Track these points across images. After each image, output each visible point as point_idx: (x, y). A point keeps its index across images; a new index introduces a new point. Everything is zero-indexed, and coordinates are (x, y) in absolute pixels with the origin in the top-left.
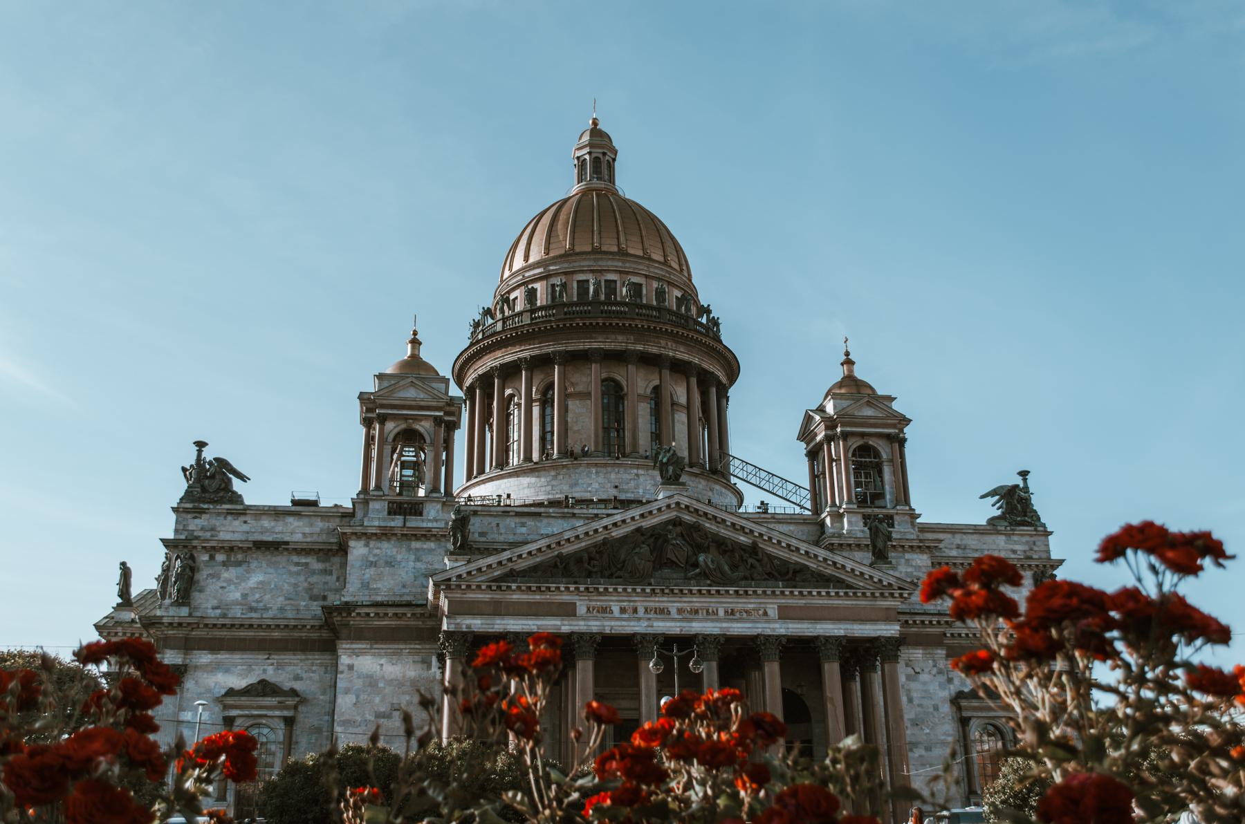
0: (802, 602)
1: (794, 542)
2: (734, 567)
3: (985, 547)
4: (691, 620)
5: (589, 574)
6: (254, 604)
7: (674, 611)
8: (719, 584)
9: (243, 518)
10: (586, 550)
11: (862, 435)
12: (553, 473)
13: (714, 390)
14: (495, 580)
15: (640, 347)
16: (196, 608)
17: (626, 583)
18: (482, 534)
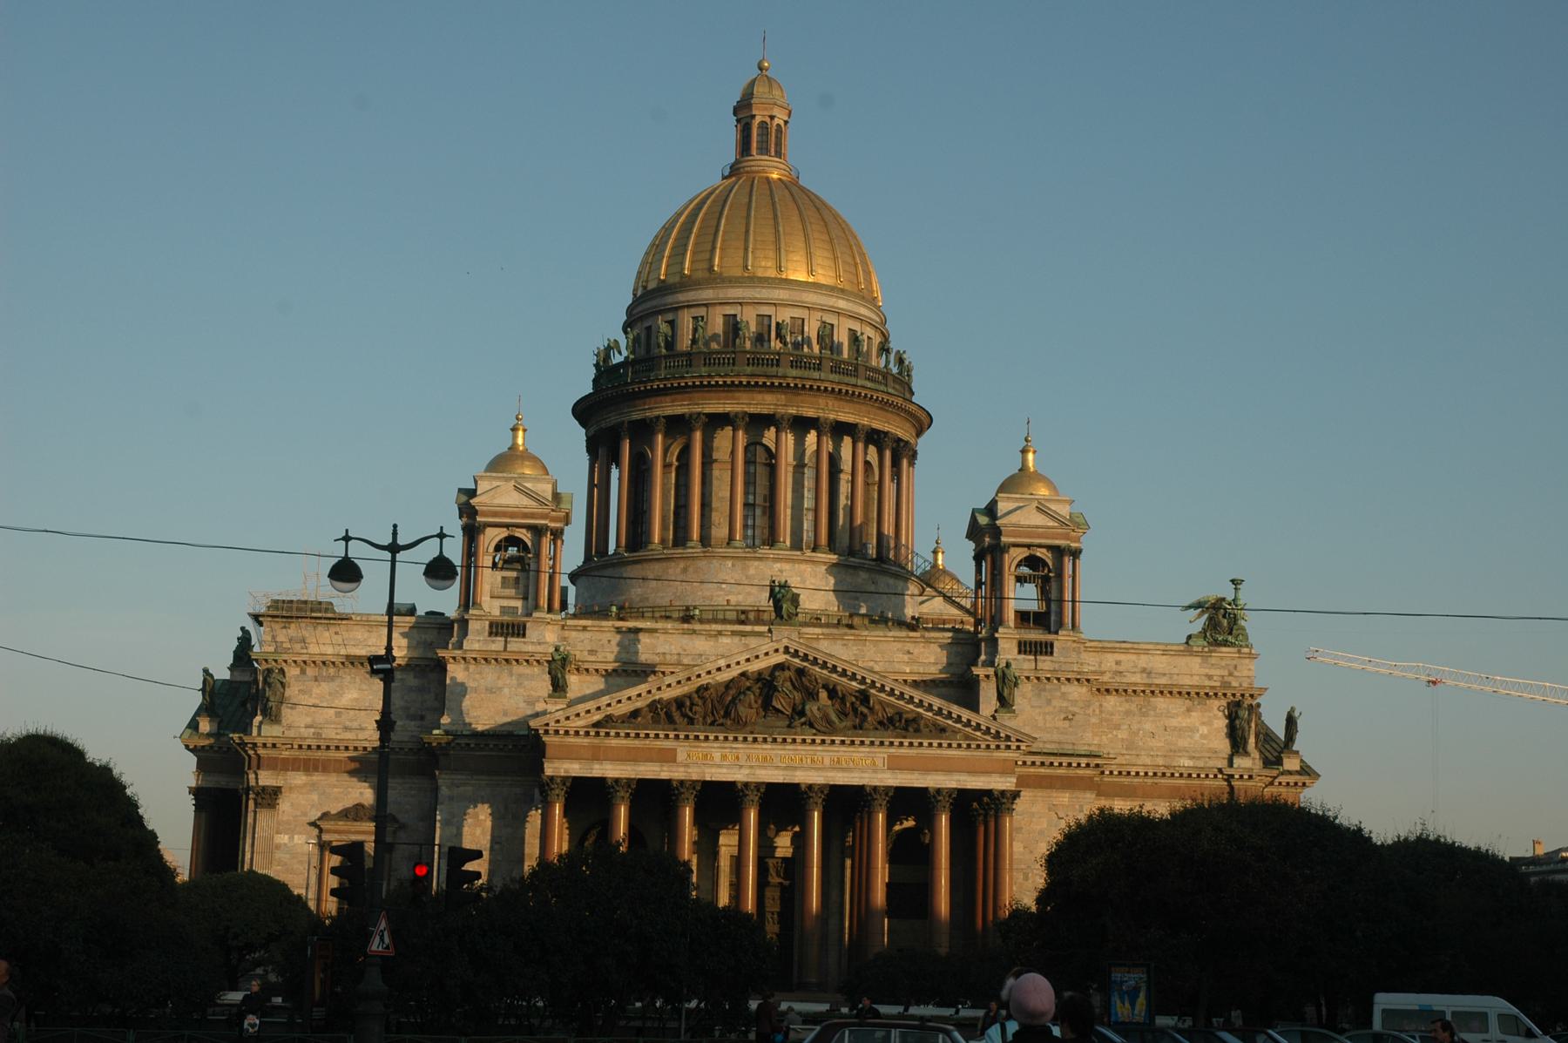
0: (913, 752)
1: (908, 691)
2: (843, 714)
3: (1175, 671)
4: (795, 768)
5: (691, 721)
6: (348, 724)
7: (777, 762)
8: (825, 733)
9: (333, 629)
10: (689, 696)
11: (1029, 546)
12: (682, 565)
13: (888, 454)
14: (597, 725)
15: (793, 411)
16: (290, 727)
17: (728, 730)
18: (592, 652)
